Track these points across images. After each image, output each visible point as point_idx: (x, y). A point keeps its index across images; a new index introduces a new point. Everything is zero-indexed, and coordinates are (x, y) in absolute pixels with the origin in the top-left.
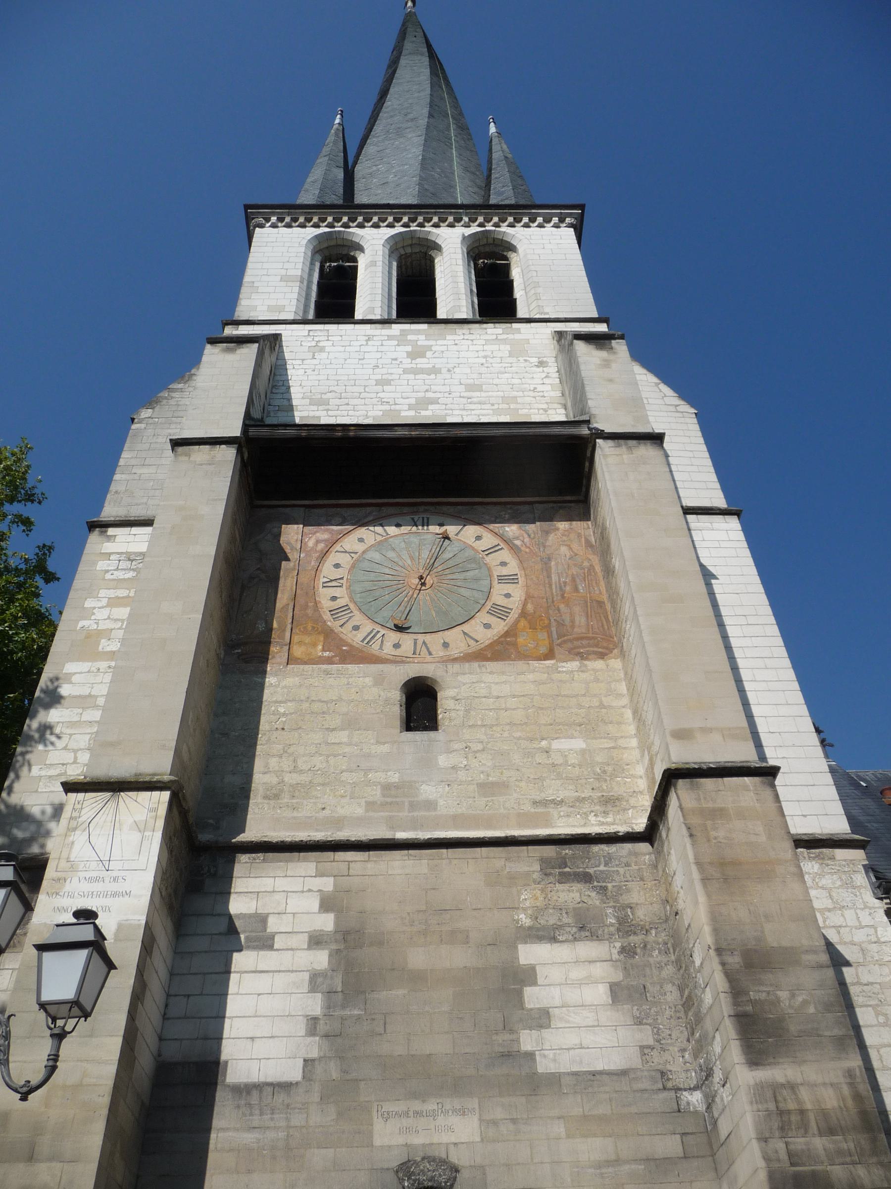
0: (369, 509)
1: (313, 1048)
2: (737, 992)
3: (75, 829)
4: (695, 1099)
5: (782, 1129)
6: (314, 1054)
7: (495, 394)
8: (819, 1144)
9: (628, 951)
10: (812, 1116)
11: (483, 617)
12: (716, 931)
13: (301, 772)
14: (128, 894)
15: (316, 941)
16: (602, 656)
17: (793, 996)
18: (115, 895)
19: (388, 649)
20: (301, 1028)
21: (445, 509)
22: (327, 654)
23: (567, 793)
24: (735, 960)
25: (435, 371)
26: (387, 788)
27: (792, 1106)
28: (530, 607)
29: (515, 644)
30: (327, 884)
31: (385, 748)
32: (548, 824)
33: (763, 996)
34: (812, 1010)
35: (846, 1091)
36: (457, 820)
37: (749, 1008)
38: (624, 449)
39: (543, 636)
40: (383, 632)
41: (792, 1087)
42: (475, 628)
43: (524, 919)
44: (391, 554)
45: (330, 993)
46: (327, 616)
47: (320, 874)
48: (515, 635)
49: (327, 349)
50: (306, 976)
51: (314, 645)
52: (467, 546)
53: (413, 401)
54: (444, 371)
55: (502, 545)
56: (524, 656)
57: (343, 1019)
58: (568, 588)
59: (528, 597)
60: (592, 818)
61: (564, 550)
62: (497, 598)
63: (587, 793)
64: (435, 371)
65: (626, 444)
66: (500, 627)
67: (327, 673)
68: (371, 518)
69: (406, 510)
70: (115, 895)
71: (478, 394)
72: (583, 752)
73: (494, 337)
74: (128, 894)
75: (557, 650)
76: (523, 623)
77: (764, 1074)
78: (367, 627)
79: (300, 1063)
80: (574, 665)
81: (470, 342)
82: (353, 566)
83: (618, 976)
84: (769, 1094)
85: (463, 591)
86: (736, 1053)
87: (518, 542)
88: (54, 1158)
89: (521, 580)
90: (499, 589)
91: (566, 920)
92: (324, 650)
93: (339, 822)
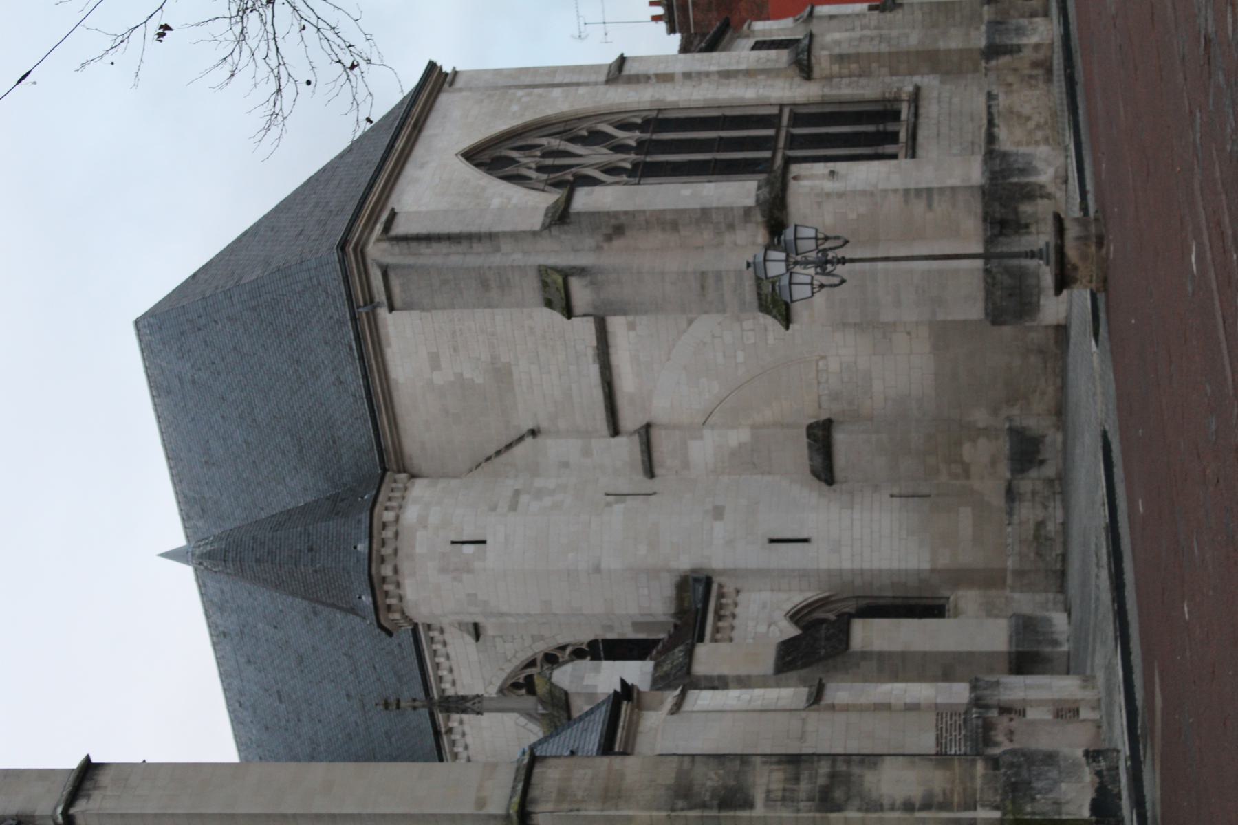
2: (704, 806)
5: (793, 801)
8: (804, 787)
10: (788, 786)
12: (658, 809)
17: (710, 779)
24: (680, 804)
27: (780, 794)
33: (708, 794)
34: (721, 772)
35: (774, 767)
37: (715, 803)
41: (768, 792)
65: (89, 790)
77: (759, 798)
84: (772, 803)
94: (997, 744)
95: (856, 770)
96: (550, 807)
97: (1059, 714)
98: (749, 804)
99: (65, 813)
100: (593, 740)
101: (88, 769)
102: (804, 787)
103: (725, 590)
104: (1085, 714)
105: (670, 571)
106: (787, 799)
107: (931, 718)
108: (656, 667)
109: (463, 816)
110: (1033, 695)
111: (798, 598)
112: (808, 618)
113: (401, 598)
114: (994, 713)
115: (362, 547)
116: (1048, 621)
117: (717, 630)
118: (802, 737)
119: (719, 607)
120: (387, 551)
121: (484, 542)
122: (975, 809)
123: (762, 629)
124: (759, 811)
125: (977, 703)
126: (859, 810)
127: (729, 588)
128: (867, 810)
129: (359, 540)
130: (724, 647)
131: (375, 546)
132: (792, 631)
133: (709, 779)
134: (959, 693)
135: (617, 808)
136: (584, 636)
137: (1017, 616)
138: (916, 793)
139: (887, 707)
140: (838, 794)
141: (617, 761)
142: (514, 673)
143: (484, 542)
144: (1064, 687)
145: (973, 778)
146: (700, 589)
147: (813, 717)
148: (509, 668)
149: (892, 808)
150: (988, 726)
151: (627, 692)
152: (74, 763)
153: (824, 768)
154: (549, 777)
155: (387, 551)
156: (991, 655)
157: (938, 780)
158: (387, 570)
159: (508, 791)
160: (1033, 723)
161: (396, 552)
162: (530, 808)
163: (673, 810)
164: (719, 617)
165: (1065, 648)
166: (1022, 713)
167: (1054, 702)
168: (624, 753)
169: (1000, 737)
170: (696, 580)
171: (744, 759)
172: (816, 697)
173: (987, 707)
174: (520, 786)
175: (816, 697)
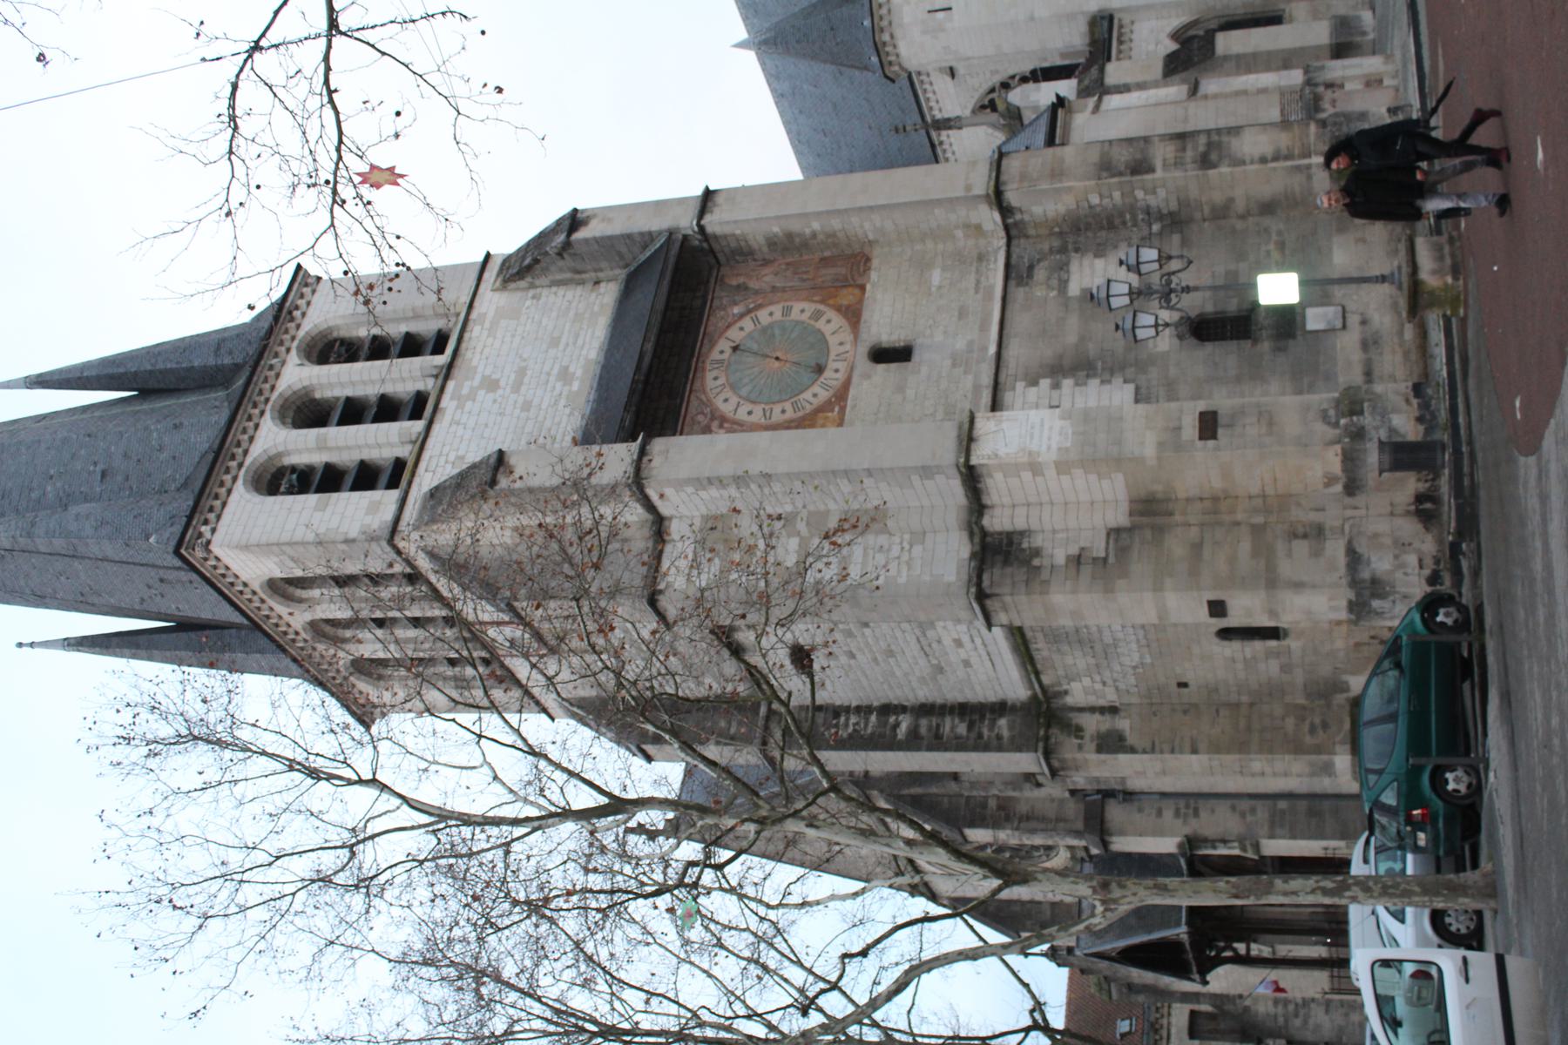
0: (692, 397)
1: (1118, 380)
2: (1121, 174)
3: (996, 455)
4: (1156, 228)
6: (1121, 380)
7: (567, 328)
8: (1189, 154)
9: (1077, 250)
11: (821, 324)
12: (1089, 179)
13: (935, 411)
14: (1042, 420)
15: (1056, 386)
16: (868, 260)
18: (1042, 425)
19: (841, 376)
20: (1107, 387)
21: (704, 350)
22: (837, 409)
23: (972, 278)
24: (1105, 174)
25: (522, 372)
26: (954, 365)
27: (1172, 161)
28: (816, 298)
29: (848, 307)
30: (1020, 385)
31: (924, 370)
32: (991, 288)
36: (984, 327)
38: (717, 210)
39: (845, 291)
40: (822, 379)
41: (1165, 160)
42: (827, 330)
43: (1054, 293)
44: (746, 380)
45: (1088, 376)
46: (800, 414)
47: (1014, 389)
48: (841, 306)
49: (461, 453)
50: (1077, 388)
51: (826, 418)
52: (750, 336)
53: (559, 385)
54: (523, 364)
55: (753, 315)
56: (861, 301)
57: (1103, 369)
58: (805, 277)
59: (808, 299)
60: (992, 266)
61: (767, 279)
62: (805, 317)
63: (974, 269)
64: (522, 372)
66: (831, 314)
67: (854, 407)
68: (703, 397)
69: (698, 375)
70: (1042, 425)
71: (564, 341)
72: (944, 269)
73: (485, 333)
74: (1042, 420)
75: (859, 282)
76: (831, 302)
77: (1158, 164)
78: (816, 389)
79: (1126, 386)
80: (874, 275)
81: (487, 351)
82: (753, 402)
83: (1090, 255)
85: (793, 336)
86: (1148, 177)
87: (752, 306)
88: (1180, 419)
89: (789, 304)
90: (795, 314)
91: (1056, 275)
92: (832, 411)
93: (977, 388)
94: (1323, 110)
95: (1225, 139)
96: (1015, 186)
97: (1368, 84)
98: (1152, 170)
99: (698, 224)
100: (1041, 137)
101: (708, 194)
102: (1189, 154)
103: (1124, 22)
104: (1387, 82)
105: (1083, 13)
106: (1178, 163)
107: (1276, 98)
108: (1080, 82)
109: (957, 198)
110: (1349, 72)
111: (1176, 22)
112: (1185, 36)
113: (898, 55)
114: (1321, 89)
115: (867, 23)
116: (1358, 18)
117: (1120, 52)
118: (1186, 120)
119: (1120, 35)
120: (884, 23)
121: (950, 9)
122: (1310, 156)
123: (1151, 47)
124: (1159, 173)
125: (1309, 82)
126: (1229, 166)
127: (1126, 21)
128: (1234, 165)
129: (864, 18)
130: (1125, 64)
131: (876, 21)
132: (1173, 46)
133: (1122, 156)
134: (1295, 77)
135: (1061, 181)
136: (1026, 67)
137: (1335, 17)
138: (1268, 150)
139: (1245, 92)
140: (1214, 157)
141: (1057, 150)
142: (982, 98)
143: (950, 9)
144: (1371, 64)
145: (1308, 135)
146: (1106, 24)
147: (1192, 105)
148: (977, 96)
149: (1252, 162)
150: (1317, 99)
151: (1060, 102)
152: (699, 192)
153: (1203, 140)
154: (1012, 166)
155: (884, 23)
156: (1318, 48)
157: (1284, 140)
158: (886, 37)
159: (986, 179)
160: (1351, 92)
161: (890, 23)
162: (1002, 188)
163: (1099, 179)
164: (1120, 42)
165: (1371, 36)
166: (1342, 86)
167: (1365, 76)
168: (1063, 144)
169: (1326, 105)
170: (1102, 18)
171: (1146, 140)
172: (1194, 91)
173: (1316, 85)
174: (994, 174)
175: (1194, 91)
